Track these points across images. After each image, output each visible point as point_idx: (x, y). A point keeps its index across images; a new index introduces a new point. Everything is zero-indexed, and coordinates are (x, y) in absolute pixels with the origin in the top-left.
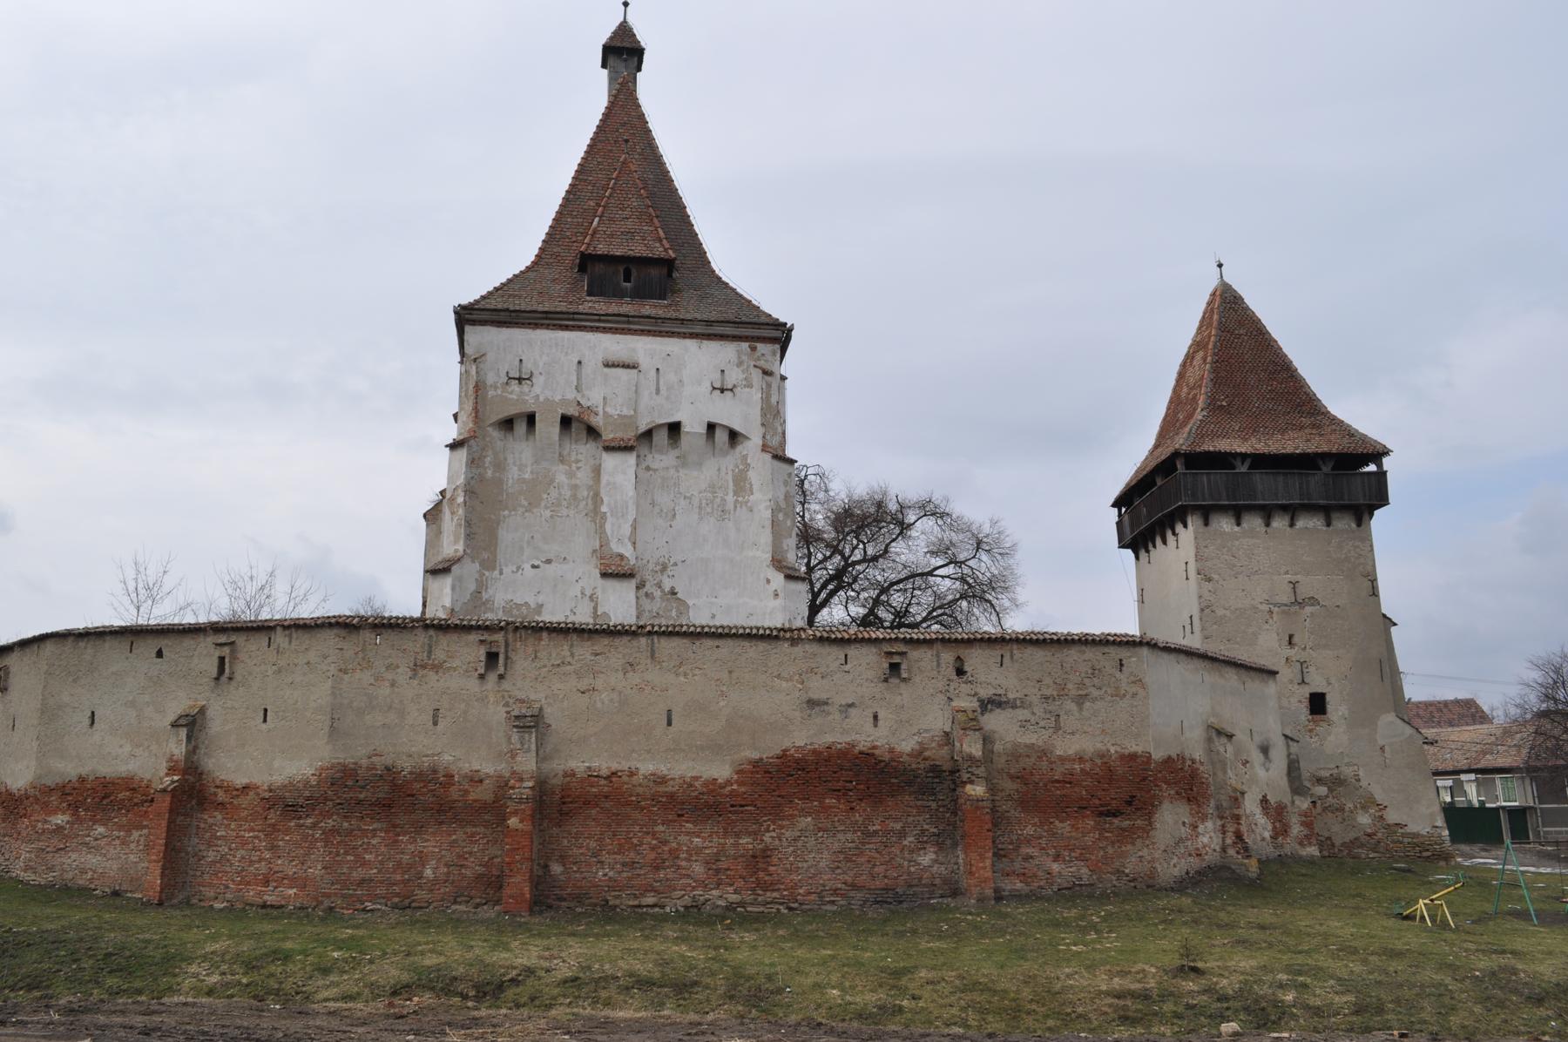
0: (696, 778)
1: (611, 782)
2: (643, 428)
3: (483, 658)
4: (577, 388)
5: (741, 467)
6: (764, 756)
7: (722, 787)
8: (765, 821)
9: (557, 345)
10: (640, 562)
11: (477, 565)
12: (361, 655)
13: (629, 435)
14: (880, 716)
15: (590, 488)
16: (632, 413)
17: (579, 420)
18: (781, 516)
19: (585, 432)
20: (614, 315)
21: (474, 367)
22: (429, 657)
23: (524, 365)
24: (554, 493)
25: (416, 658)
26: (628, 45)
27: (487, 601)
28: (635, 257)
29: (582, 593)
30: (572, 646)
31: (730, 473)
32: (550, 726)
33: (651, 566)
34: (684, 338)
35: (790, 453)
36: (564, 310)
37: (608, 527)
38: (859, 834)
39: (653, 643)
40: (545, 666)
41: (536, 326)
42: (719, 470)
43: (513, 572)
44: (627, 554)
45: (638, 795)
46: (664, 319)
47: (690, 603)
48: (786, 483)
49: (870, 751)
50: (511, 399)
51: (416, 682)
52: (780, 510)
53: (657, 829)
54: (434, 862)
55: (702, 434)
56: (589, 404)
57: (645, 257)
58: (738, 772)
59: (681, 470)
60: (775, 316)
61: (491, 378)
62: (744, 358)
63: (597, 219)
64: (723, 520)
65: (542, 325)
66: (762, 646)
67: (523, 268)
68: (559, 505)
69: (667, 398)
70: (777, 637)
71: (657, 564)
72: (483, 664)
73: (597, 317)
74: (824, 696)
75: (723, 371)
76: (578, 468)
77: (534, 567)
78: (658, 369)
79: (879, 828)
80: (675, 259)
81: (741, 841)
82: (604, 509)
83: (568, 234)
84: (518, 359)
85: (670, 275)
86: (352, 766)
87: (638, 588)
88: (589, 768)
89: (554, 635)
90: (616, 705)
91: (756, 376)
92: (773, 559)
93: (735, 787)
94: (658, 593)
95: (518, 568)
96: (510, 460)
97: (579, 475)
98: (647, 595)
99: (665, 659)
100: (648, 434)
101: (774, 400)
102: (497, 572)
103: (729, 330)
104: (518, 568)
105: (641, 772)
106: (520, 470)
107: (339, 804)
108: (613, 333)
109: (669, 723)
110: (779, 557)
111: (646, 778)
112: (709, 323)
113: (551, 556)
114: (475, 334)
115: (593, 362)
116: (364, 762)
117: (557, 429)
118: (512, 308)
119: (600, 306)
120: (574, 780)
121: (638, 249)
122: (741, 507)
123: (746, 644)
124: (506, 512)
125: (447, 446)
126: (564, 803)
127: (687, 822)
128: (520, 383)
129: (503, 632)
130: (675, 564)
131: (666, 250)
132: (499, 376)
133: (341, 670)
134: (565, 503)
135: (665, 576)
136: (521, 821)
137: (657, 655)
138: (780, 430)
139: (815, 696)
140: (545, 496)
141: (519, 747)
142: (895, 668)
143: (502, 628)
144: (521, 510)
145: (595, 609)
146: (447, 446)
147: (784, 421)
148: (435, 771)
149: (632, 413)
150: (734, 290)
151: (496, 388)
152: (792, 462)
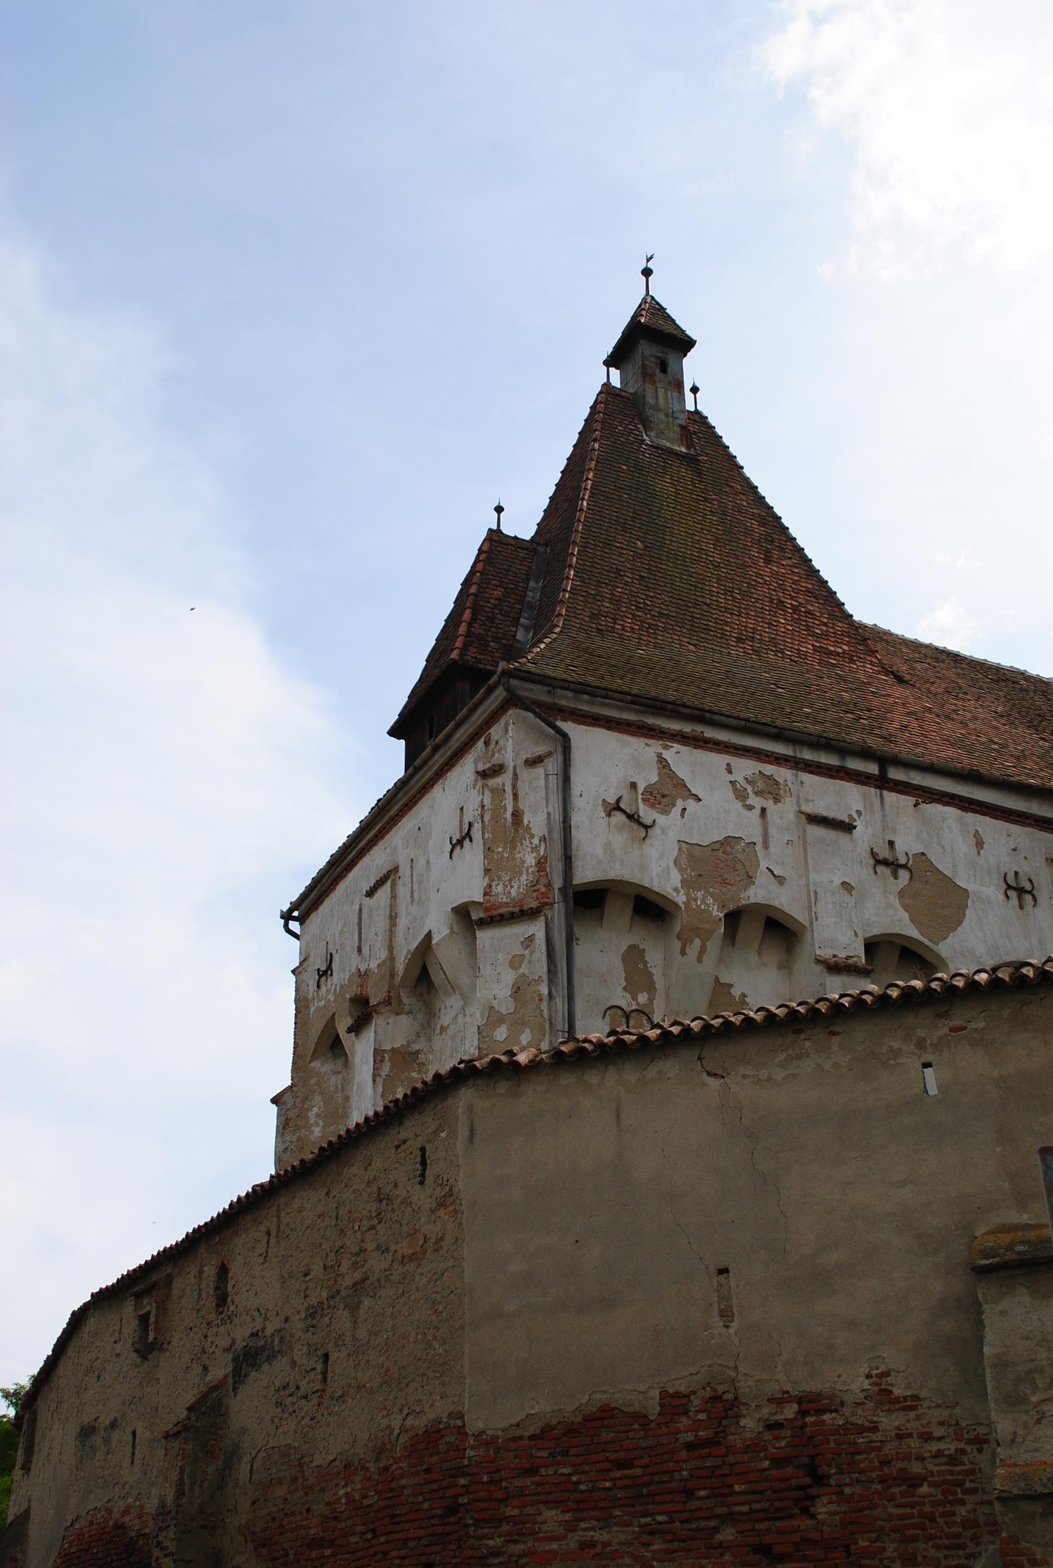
48: (515, 962)
52: (501, 1020)
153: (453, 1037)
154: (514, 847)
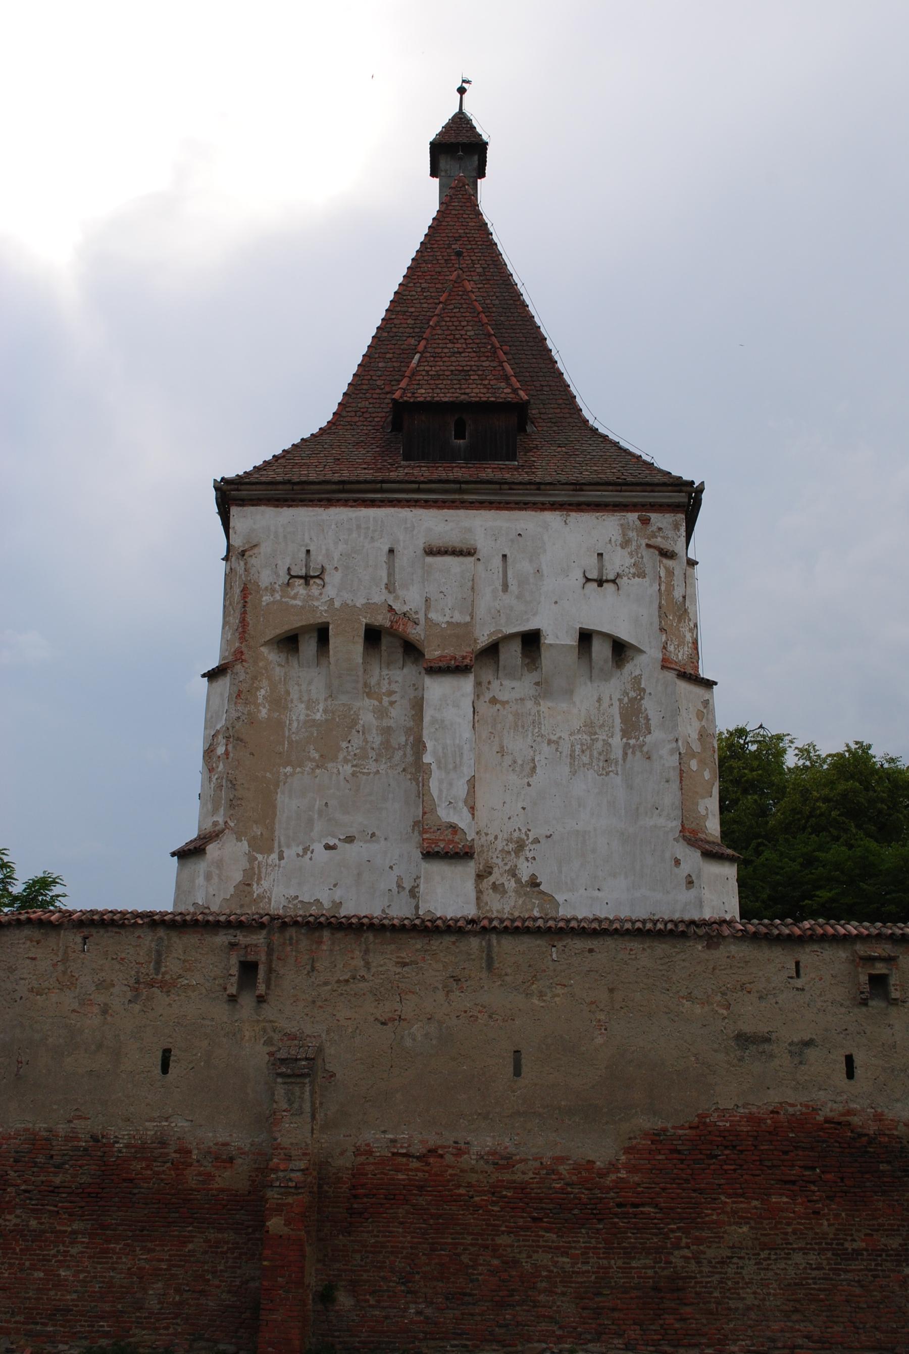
0: (561, 1160)
1: (428, 1164)
2: (483, 638)
3: (234, 971)
4: (390, 587)
5: (632, 694)
6: (669, 1125)
7: (602, 1174)
8: (672, 1231)
9: (359, 527)
10: (483, 839)
11: (244, 846)
12: (60, 968)
13: (464, 651)
14: (858, 1061)
15: (408, 731)
16: (468, 619)
17: (392, 632)
18: (694, 765)
19: (401, 650)
20: (440, 481)
21: (242, 563)
22: (157, 970)
23: (312, 558)
24: (357, 741)
25: (137, 972)
26: (463, 139)
27: (261, 897)
28: (470, 403)
29: (399, 886)
30: (367, 951)
31: (616, 704)
32: (333, 1075)
33: (500, 844)
34: (542, 510)
35: (705, 672)
36: (369, 477)
37: (434, 785)
38: (829, 1254)
39: (490, 946)
40: (326, 984)
41: (329, 503)
42: (599, 700)
43: (298, 855)
44: (462, 825)
45: (470, 1185)
46: (512, 484)
47: (560, 898)
49: (842, 1119)
50: (296, 606)
51: (137, 1007)
52: (693, 755)
53: (499, 1241)
54: (160, 1285)
55: (571, 646)
56: (405, 608)
57: (486, 402)
58: (628, 1151)
59: (542, 702)
60: (675, 473)
61: (265, 578)
62: (632, 534)
63: (417, 356)
64: (607, 774)
65: (338, 500)
66: (662, 948)
67: (315, 430)
68: (365, 757)
69: (518, 597)
70: (683, 934)
71: (509, 840)
72: (234, 979)
73: (415, 486)
74: (762, 1028)
75: (600, 555)
76: (392, 703)
77: (328, 847)
78: (504, 556)
79: (864, 1245)
80: (528, 402)
81: (634, 1264)
82: (427, 759)
83: (379, 383)
84: (304, 550)
85: (522, 429)
86: (44, 1134)
87: (480, 877)
88: (393, 1141)
89: (339, 935)
90: (434, 1042)
91: (649, 558)
92: (683, 829)
93: (623, 1174)
94: (511, 885)
95: (306, 850)
96: (294, 695)
97: (393, 712)
98: (495, 887)
99: (509, 971)
100: (492, 651)
101: (678, 594)
102: (274, 856)
103: (608, 496)
104: (306, 850)
105: (474, 1149)
106: (307, 708)
107: (26, 1191)
108: (440, 507)
109: (517, 1072)
110: (693, 826)
111: (482, 1158)
112: (579, 486)
113: (352, 831)
114: (241, 517)
115: (410, 550)
116: (62, 1129)
117: (358, 647)
118: (296, 479)
119: (422, 471)
120: (371, 1160)
121: (476, 392)
122: (634, 753)
123: (636, 945)
124: (289, 769)
125: (204, 676)
126: (355, 1196)
127: (548, 1230)
128: (307, 583)
129: (264, 932)
130: (536, 841)
131: (515, 391)
132: (278, 576)
133: (31, 990)
134: (372, 754)
135: (522, 859)
136: (288, 1223)
137: (496, 965)
138: (689, 637)
139: (747, 1028)
140: (344, 745)
141: (285, 1106)
142: (879, 983)
143: (262, 926)
144: (309, 765)
145: (417, 908)
146: (204, 676)
147: (696, 626)
148: (163, 1144)
149: (468, 619)
150: (616, 444)
151: (273, 591)
152: (709, 684)
153: (517, 715)
154: (679, 621)
